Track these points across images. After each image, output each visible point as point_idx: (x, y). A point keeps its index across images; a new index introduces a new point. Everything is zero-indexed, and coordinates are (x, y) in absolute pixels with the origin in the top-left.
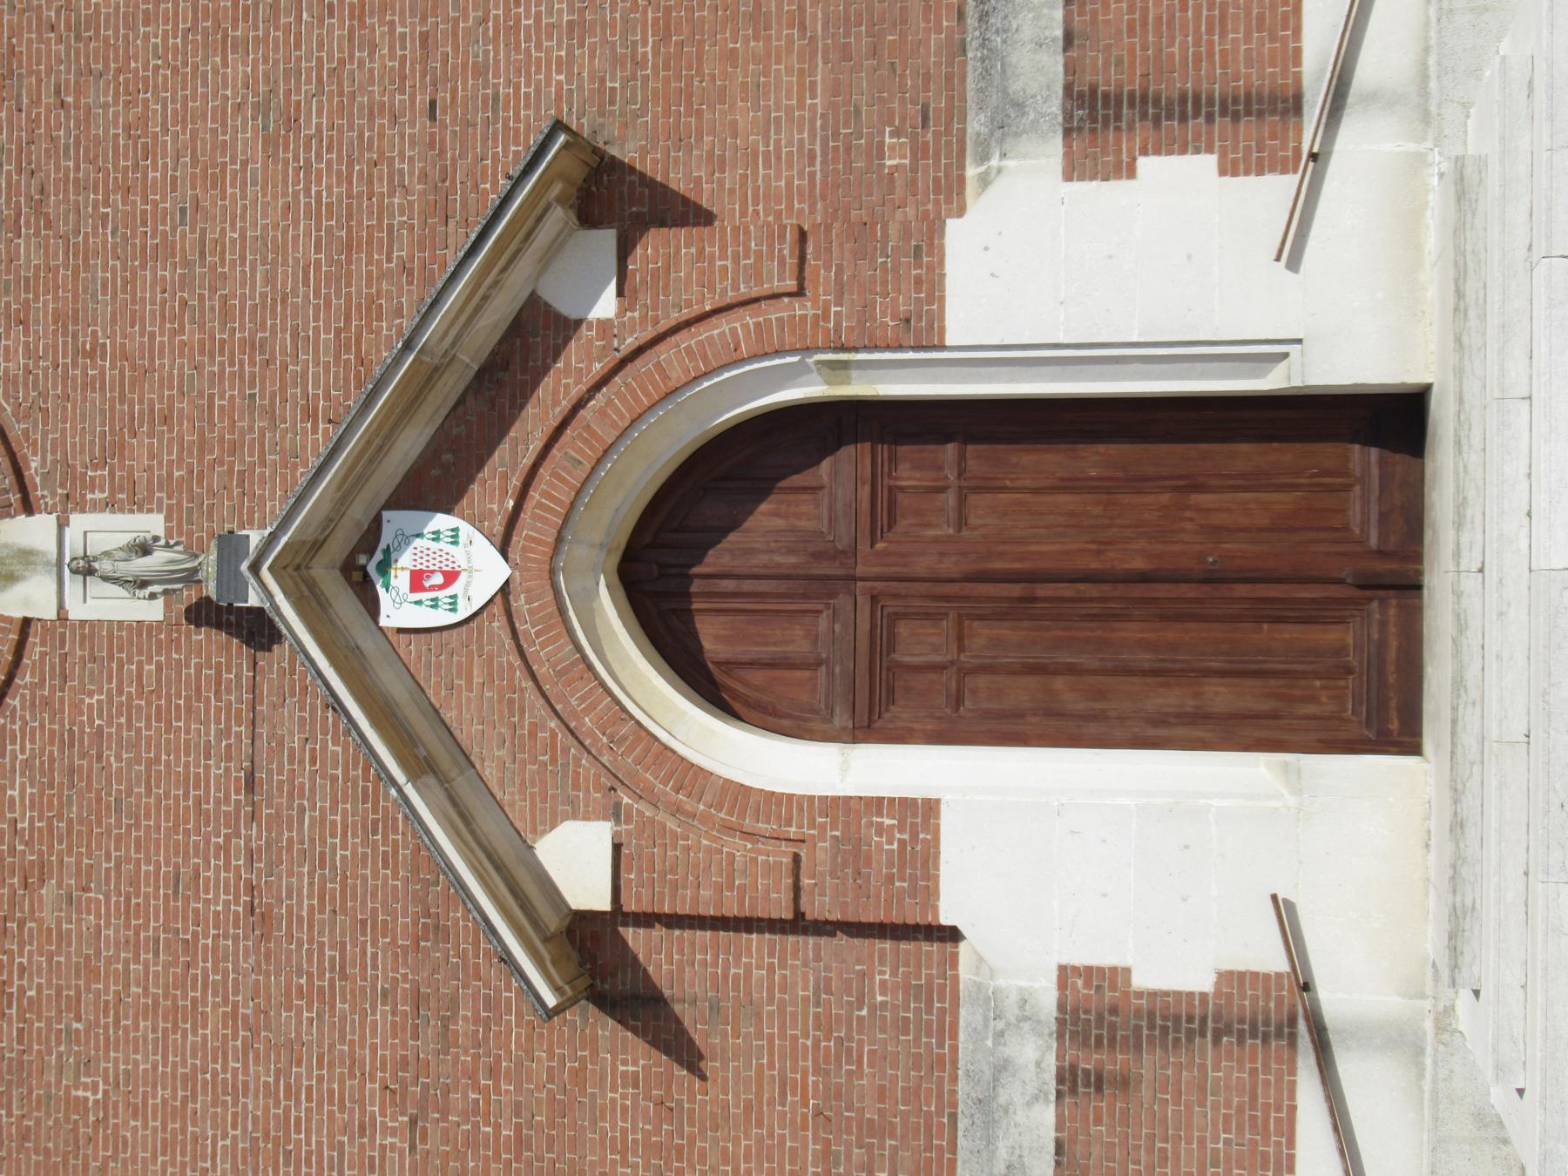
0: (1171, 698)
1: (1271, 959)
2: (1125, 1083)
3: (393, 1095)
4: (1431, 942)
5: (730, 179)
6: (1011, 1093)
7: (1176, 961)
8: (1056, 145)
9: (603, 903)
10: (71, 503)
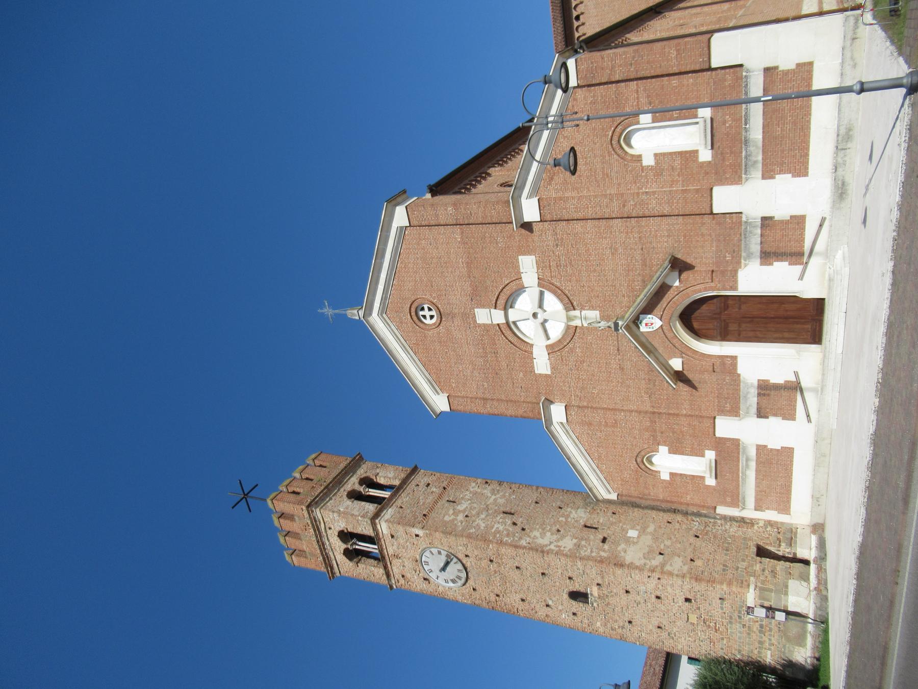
1: (793, 379)
2: (768, 395)
3: (646, 393)
4: (820, 377)
5: (698, 261)
7: (778, 378)
8: (758, 260)
9: (680, 369)
10: (582, 309)
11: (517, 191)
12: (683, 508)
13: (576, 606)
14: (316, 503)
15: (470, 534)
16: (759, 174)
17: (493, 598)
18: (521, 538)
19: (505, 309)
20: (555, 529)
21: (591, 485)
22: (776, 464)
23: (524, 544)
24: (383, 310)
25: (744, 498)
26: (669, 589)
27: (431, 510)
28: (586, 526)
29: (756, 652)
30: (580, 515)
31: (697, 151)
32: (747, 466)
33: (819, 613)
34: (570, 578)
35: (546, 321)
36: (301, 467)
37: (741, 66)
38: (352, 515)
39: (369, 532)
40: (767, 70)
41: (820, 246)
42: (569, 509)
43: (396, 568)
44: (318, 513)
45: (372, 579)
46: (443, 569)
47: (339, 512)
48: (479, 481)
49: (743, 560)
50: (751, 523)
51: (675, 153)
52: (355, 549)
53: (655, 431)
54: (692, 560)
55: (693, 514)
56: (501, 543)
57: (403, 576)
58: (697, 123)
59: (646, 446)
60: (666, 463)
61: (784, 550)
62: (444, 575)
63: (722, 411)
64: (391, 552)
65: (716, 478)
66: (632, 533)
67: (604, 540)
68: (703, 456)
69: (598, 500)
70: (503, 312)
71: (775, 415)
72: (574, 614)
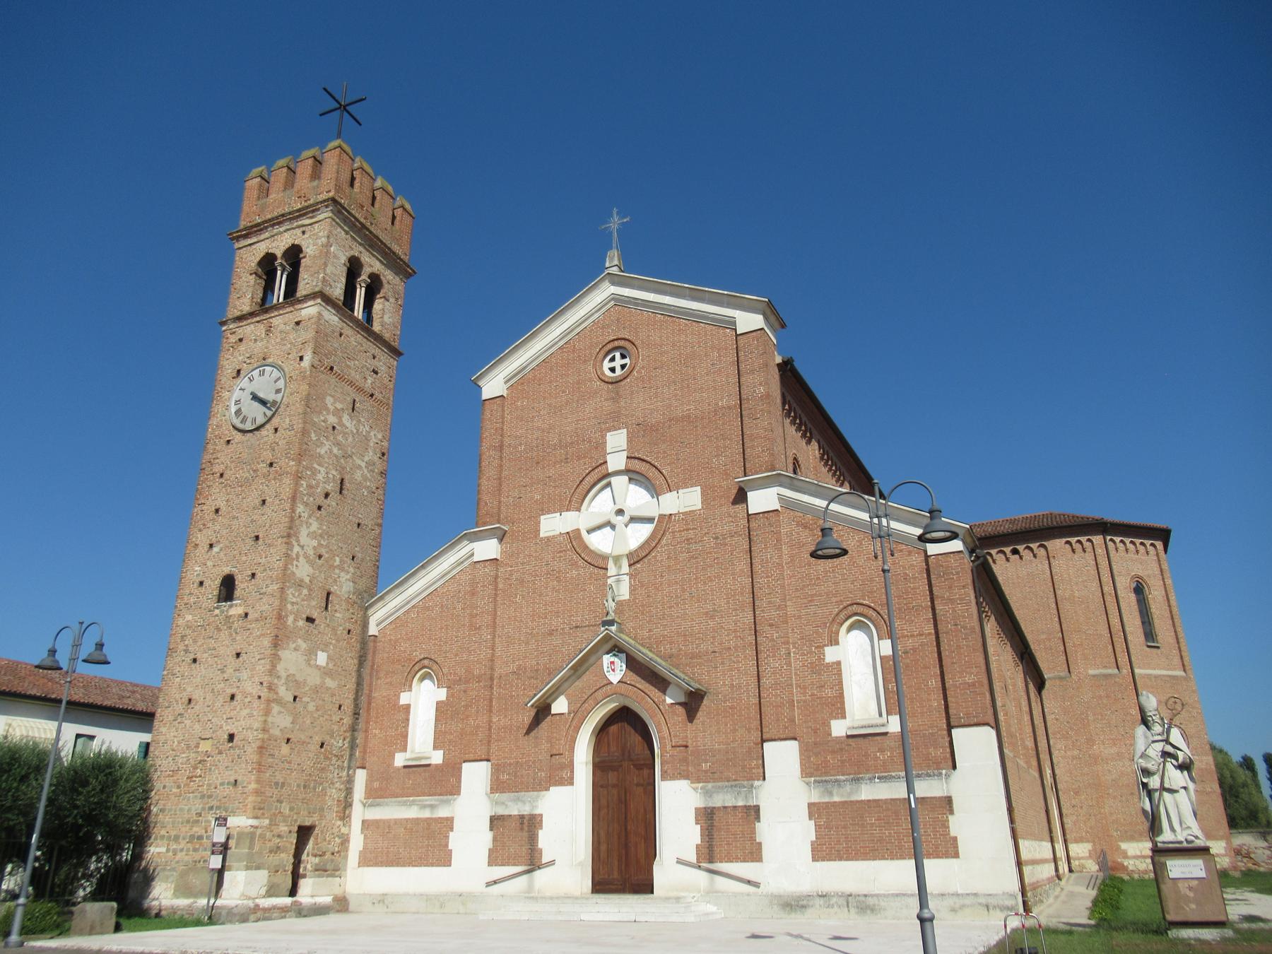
0: (602, 834)
3: (519, 667)
4: (548, 894)
6: (520, 804)
7: (546, 840)
8: (701, 805)
9: (553, 712)
10: (631, 575)
11: (788, 480)
12: (361, 725)
13: (213, 585)
14: (339, 212)
15: (309, 433)
16: (816, 797)
17: (218, 469)
18: (306, 504)
19: (627, 471)
20: (323, 551)
21: (387, 598)
22: (429, 845)
23: (298, 510)
24: (619, 301)
25: (378, 805)
26: (245, 712)
27: (341, 378)
28: (328, 594)
29: (163, 832)
30: (344, 586)
31: (844, 717)
32: (424, 807)
33: (224, 913)
34: (253, 575)
35: (613, 527)
36: (390, 188)
37: (954, 767)
38: (325, 265)
39: (303, 289)
40: (948, 801)
41: (721, 882)
42: (352, 570)
43: (251, 330)
44: (325, 214)
45: (234, 296)
46: (255, 397)
47: (328, 245)
48: (385, 444)
49: (291, 809)
50: (345, 815)
51: (842, 689)
52: (276, 270)
53: (467, 682)
54: (288, 740)
55: (353, 740)
56: (298, 477)
57: (241, 340)
58: (880, 715)
59: (445, 670)
60: (424, 699)
61: (309, 861)
62: (246, 398)
63: (497, 770)
64: (276, 321)
65: (405, 767)
66: (322, 659)
67: (310, 620)
68: (435, 748)
69: (367, 609)
70: (623, 467)
71: (495, 840)
72: (201, 583)
